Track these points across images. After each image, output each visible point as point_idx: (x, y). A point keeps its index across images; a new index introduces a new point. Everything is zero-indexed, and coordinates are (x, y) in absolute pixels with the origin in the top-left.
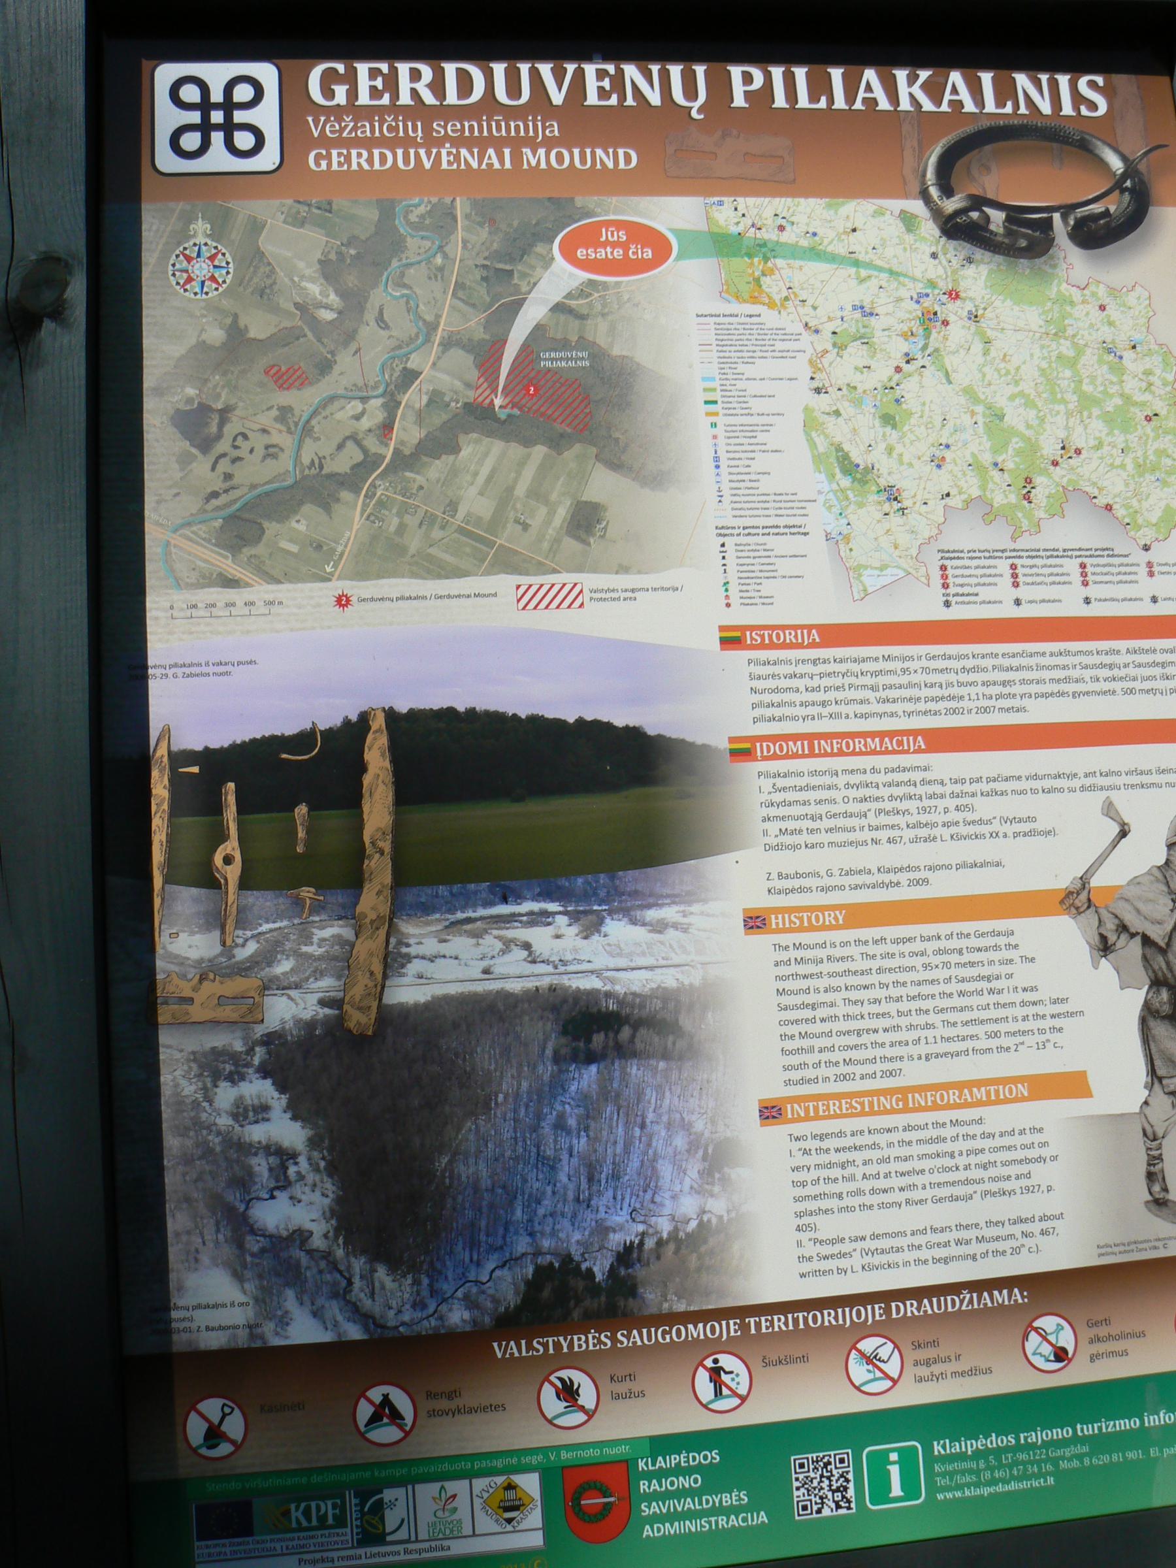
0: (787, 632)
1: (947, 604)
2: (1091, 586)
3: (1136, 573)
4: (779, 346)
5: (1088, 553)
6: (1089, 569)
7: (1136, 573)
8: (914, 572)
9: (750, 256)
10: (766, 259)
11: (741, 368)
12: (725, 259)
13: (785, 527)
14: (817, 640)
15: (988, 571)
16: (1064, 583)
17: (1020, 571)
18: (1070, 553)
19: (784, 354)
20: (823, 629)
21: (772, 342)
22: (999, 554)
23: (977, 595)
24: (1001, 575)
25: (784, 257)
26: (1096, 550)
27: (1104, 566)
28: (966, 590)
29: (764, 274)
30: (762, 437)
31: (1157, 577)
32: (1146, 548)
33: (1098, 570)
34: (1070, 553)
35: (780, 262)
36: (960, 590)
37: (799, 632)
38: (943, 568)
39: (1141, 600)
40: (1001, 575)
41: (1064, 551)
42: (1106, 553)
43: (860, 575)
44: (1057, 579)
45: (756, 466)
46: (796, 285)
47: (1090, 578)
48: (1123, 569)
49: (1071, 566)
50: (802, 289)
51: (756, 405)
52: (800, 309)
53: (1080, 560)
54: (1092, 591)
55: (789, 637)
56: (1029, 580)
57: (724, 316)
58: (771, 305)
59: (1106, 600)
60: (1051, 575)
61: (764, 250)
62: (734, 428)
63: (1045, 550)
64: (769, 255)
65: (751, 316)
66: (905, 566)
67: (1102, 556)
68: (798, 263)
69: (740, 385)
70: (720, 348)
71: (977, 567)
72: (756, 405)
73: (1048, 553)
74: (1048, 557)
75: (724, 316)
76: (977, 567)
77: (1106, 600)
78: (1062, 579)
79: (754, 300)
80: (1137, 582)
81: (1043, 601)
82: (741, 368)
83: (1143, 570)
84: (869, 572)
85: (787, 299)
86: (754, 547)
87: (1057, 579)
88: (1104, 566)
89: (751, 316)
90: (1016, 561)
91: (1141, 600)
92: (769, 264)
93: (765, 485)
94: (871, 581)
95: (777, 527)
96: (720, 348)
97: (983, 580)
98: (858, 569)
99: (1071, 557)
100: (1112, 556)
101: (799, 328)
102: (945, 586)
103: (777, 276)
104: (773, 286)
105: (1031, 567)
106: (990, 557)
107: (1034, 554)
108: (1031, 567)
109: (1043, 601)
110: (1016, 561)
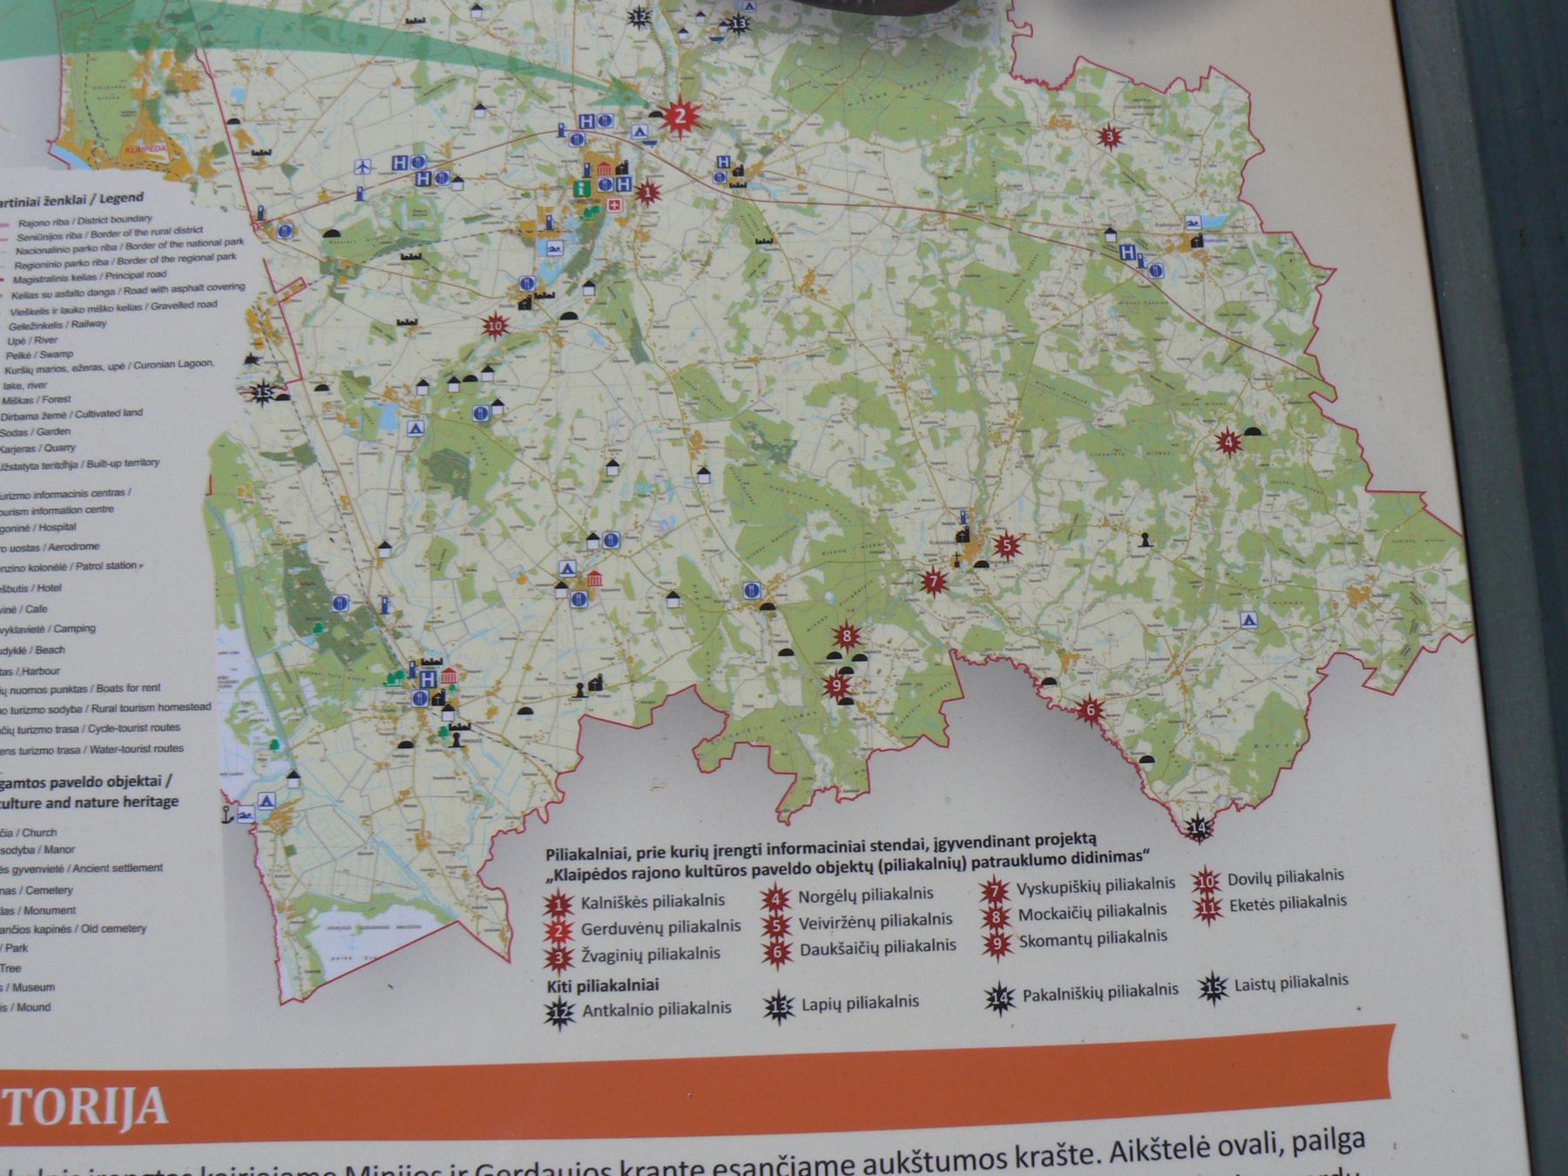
0: (77, 1092)
1: (559, 1015)
2: (1018, 955)
3: (1161, 910)
4: (179, 274)
5: (1014, 853)
6: (1014, 903)
7: (1161, 910)
8: (466, 918)
9: (143, 45)
10: (184, 50)
11: (67, 338)
12: (82, 57)
13: (117, 782)
14: (161, 1119)
15: (693, 915)
16: (932, 946)
17: (795, 911)
18: (957, 854)
19: (187, 297)
20: (176, 1084)
21: (159, 267)
22: (736, 861)
23: (653, 986)
24: (735, 927)
25: (232, 44)
26: (1040, 842)
27: (1062, 890)
28: (622, 972)
29: (172, 90)
30: (88, 528)
31: (1228, 920)
32: (1199, 831)
33: (1042, 903)
34: (957, 854)
35: (219, 57)
36: (602, 972)
37: (111, 1092)
38: (558, 905)
39: (1172, 990)
40: (735, 927)
41: (940, 846)
42: (1070, 850)
43: (307, 925)
44: (909, 934)
45: (61, 609)
46: (250, 112)
47: (1015, 929)
48: (1121, 899)
49: (959, 895)
50: (266, 122)
51: (89, 439)
52: (250, 176)
53: (985, 875)
54: (1017, 970)
55: (81, 1108)
56: (822, 938)
57: (50, 202)
58: (173, 171)
59: (1058, 995)
60: (894, 921)
61: (182, 27)
62: (19, 504)
63: (879, 846)
64: (194, 40)
65: (116, 200)
66: (443, 899)
67: (1061, 860)
68: (264, 56)
69: (57, 384)
70: (22, 288)
71: (659, 903)
72: (89, 439)
73: (889, 857)
74: (887, 868)
75: (50, 202)
76: (659, 903)
77: (1058, 995)
78: (924, 934)
79: (133, 158)
80: (1162, 937)
81: (861, 1003)
82: (67, 338)
83: (1184, 899)
84: (335, 916)
85: (219, 150)
86: (19, 842)
87: (909, 934)
88: (1062, 890)
89: (116, 200)
90: (787, 883)
91: (1172, 990)
92: (192, 64)
93: (82, 663)
94: (336, 943)
95: (92, 782)
96: (22, 288)
97: (673, 943)
98: (298, 914)
99: (959, 866)
100: (1091, 858)
101: (239, 224)
102: (559, 960)
103: (207, 93)
104: (189, 122)
105: (831, 899)
106: (708, 871)
107: (844, 858)
108: (831, 899)
109: (861, 1003)
110: (787, 883)
